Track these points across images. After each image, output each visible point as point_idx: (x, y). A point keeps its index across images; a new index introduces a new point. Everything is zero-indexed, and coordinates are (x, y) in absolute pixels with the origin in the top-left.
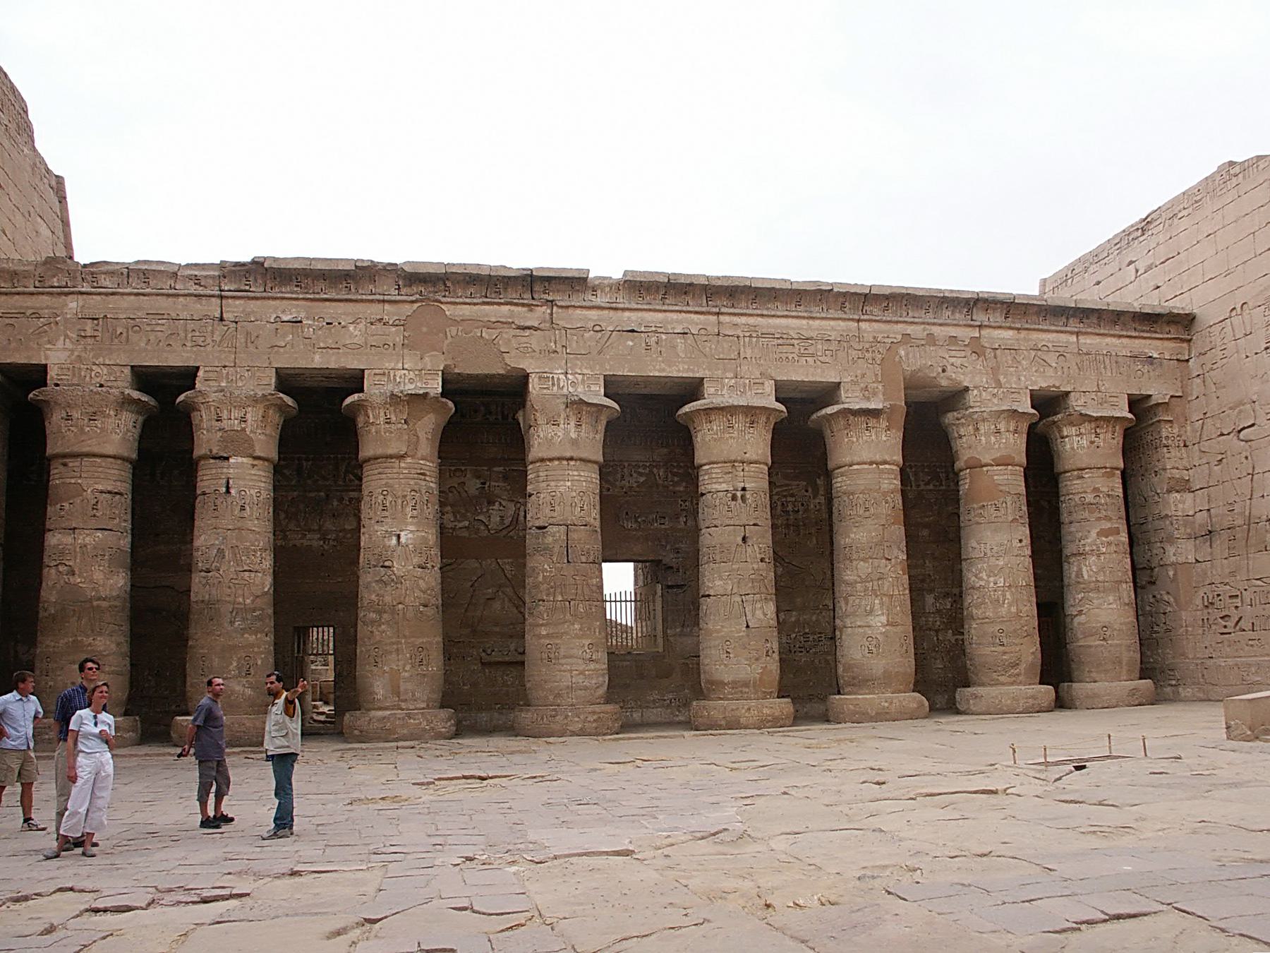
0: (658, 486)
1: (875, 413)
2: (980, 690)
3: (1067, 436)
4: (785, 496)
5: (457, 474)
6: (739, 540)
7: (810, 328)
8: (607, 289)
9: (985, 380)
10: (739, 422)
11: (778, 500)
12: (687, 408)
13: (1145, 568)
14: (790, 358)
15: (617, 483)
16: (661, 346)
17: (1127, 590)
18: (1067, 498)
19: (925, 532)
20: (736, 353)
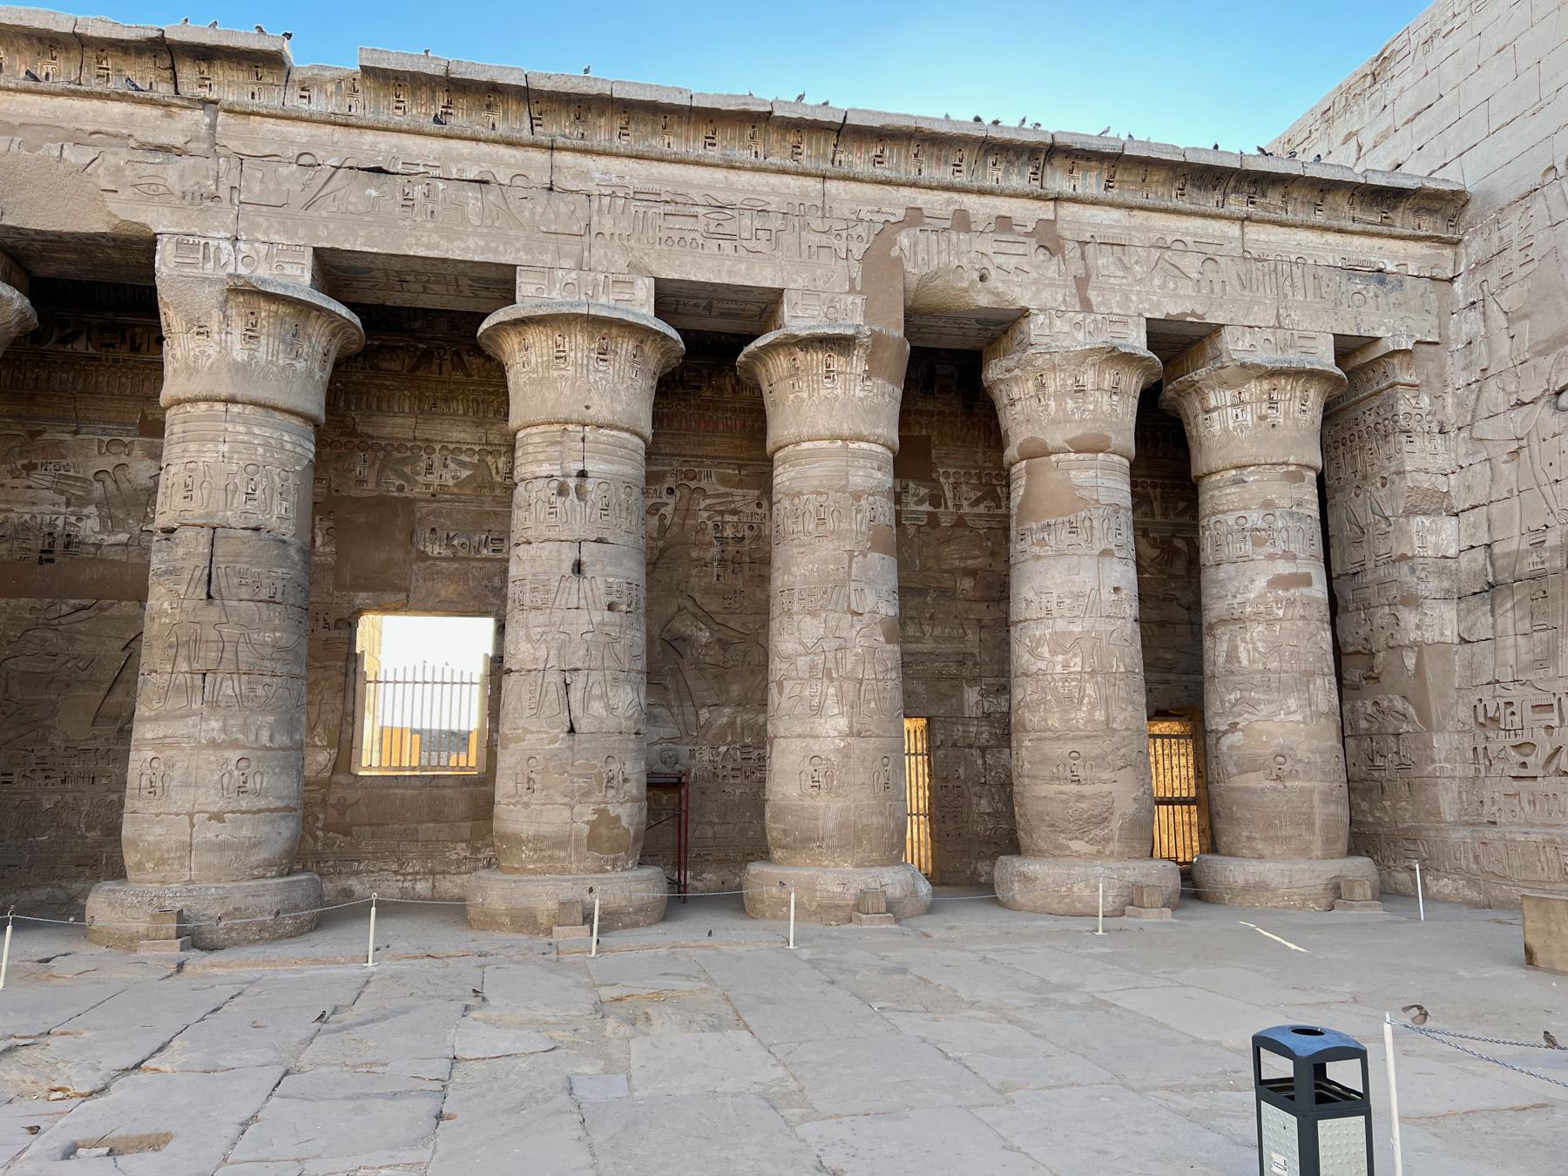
0: (492, 486)
1: (839, 344)
2: (1032, 867)
3: (1216, 408)
4: (721, 513)
5: (114, 449)
6: (567, 567)
7: (730, 187)
8: (331, 88)
9: (1060, 298)
10: (579, 345)
11: (709, 518)
12: (485, 325)
13: (1359, 652)
14: (688, 240)
15: (417, 478)
16: (435, 202)
17: (1324, 691)
18: (1214, 519)
19: (967, 584)
20: (583, 224)
